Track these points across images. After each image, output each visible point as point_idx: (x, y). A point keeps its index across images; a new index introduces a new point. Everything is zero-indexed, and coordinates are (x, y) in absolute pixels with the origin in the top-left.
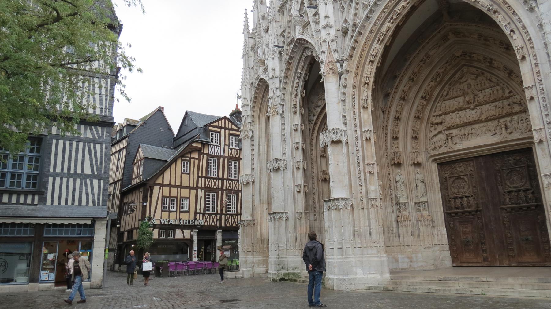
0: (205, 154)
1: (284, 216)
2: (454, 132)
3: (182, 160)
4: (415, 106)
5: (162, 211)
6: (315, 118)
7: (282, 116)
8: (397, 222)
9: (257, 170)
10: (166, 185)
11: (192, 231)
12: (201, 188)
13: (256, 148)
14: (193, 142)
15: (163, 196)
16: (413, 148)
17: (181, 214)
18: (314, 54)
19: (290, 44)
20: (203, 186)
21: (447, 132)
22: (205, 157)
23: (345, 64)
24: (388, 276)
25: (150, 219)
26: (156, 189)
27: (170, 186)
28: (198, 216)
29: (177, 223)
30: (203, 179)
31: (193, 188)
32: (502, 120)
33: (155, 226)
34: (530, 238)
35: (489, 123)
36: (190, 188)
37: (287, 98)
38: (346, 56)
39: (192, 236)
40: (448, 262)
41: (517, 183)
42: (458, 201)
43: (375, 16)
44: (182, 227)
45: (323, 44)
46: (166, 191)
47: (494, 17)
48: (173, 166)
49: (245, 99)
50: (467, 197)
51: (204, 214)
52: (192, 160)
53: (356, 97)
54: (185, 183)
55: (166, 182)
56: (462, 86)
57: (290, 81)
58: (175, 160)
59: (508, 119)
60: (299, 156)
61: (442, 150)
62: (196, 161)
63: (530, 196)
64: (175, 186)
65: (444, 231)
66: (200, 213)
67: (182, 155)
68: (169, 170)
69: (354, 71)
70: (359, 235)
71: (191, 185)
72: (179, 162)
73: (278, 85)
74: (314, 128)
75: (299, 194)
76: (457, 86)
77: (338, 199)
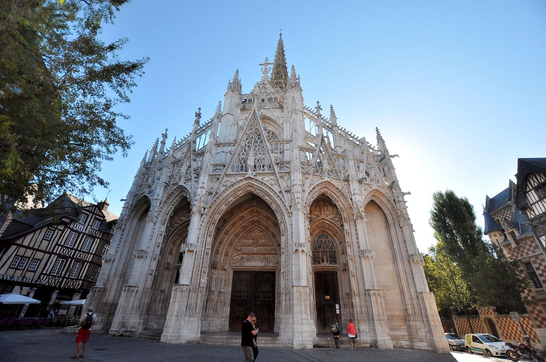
0: (70, 228)
1: (136, 289)
2: (245, 256)
4: (230, 239)
5: (9, 268)
6: (173, 230)
7: (155, 224)
8: (207, 301)
9: (119, 252)
10: (24, 247)
12: (55, 254)
13: (124, 238)
14: (64, 217)
15: (16, 255)
16: (224, 260)
17: (28, 272)
18: (188, 196)
19: (174, 184)
21: (242, 256)
22: (69, 230)
23: (206, 210)
24: (199, 335)
27: (28, 247)
28: (42, 276)
31: (48, 253)
32: (266, 256)
34: (267, 317)
35: (261, 256)
36: (45, 252)
37: (161, 214)
38: (208, 206)
40: (227, 328)
41: (266, 288)
42: (239, 293)
43: (228, 192)
45: (198, 196)
47: (276, 213)
48: (38, 232)
49: (128, 203)
50: (244, 292)
52: (57, 231)
53: (207, 229)
56: (253, 235)
57: (167, 205)
59: (269, 256)
60: (158, 251)
61: (237, 264)
62: (60, 232)
63: (271, 295)
64: (33, 249)
65: (228, 309)
68: (32, 234)
69: (210, 215)
70: (189, 309)
72: (44, 230)
73: (158, 204)
74: (171, 235)
75: (151, 276)
76: (251, 234)
77: (183, 285)
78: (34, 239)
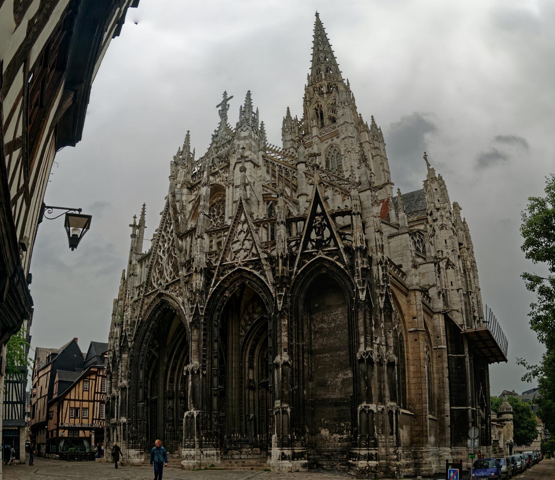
0: (101, 376)
3: (84, 381)
5: (70, 418)
10: (72, 400)
11: (91, 432)
12: (97, 401)
14: (91, 368)
15: (70, 408)
20: (99, 399)
22: (100, 378)
25: (62, 424)
26: (66, 402)
27: (75, 400)
28: (94, 421)
29: (80, 426)
30: (99, 395)
31: (91, 401)
33: (65, 428)
36: (89, 401)
39: (91, 435)
44: (84, 429)
46: (72, 404)
48: (77, 386)
51: (99, 419)
52: (91, 381)
54: (86, 398)
55: (72, 398)
58: (78, 382)
62: (94, 381)
64: (78, 400)
66: (96, 419)
67: (83, 378)
68: (74, 389)
71: (90, 399)
72: (81, 383)
78: (77, 392)
